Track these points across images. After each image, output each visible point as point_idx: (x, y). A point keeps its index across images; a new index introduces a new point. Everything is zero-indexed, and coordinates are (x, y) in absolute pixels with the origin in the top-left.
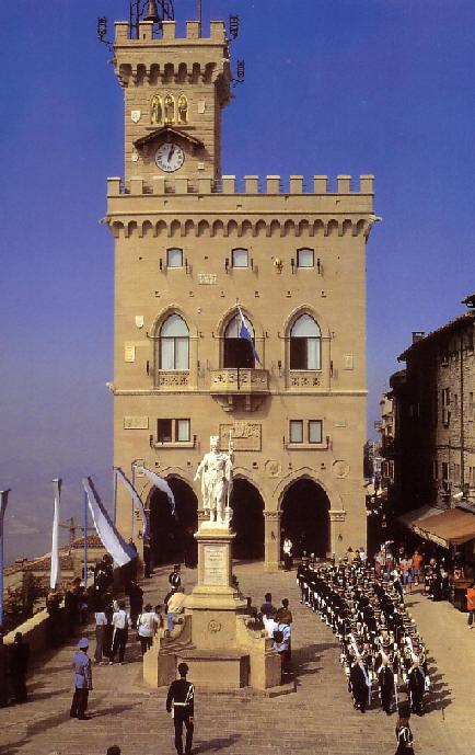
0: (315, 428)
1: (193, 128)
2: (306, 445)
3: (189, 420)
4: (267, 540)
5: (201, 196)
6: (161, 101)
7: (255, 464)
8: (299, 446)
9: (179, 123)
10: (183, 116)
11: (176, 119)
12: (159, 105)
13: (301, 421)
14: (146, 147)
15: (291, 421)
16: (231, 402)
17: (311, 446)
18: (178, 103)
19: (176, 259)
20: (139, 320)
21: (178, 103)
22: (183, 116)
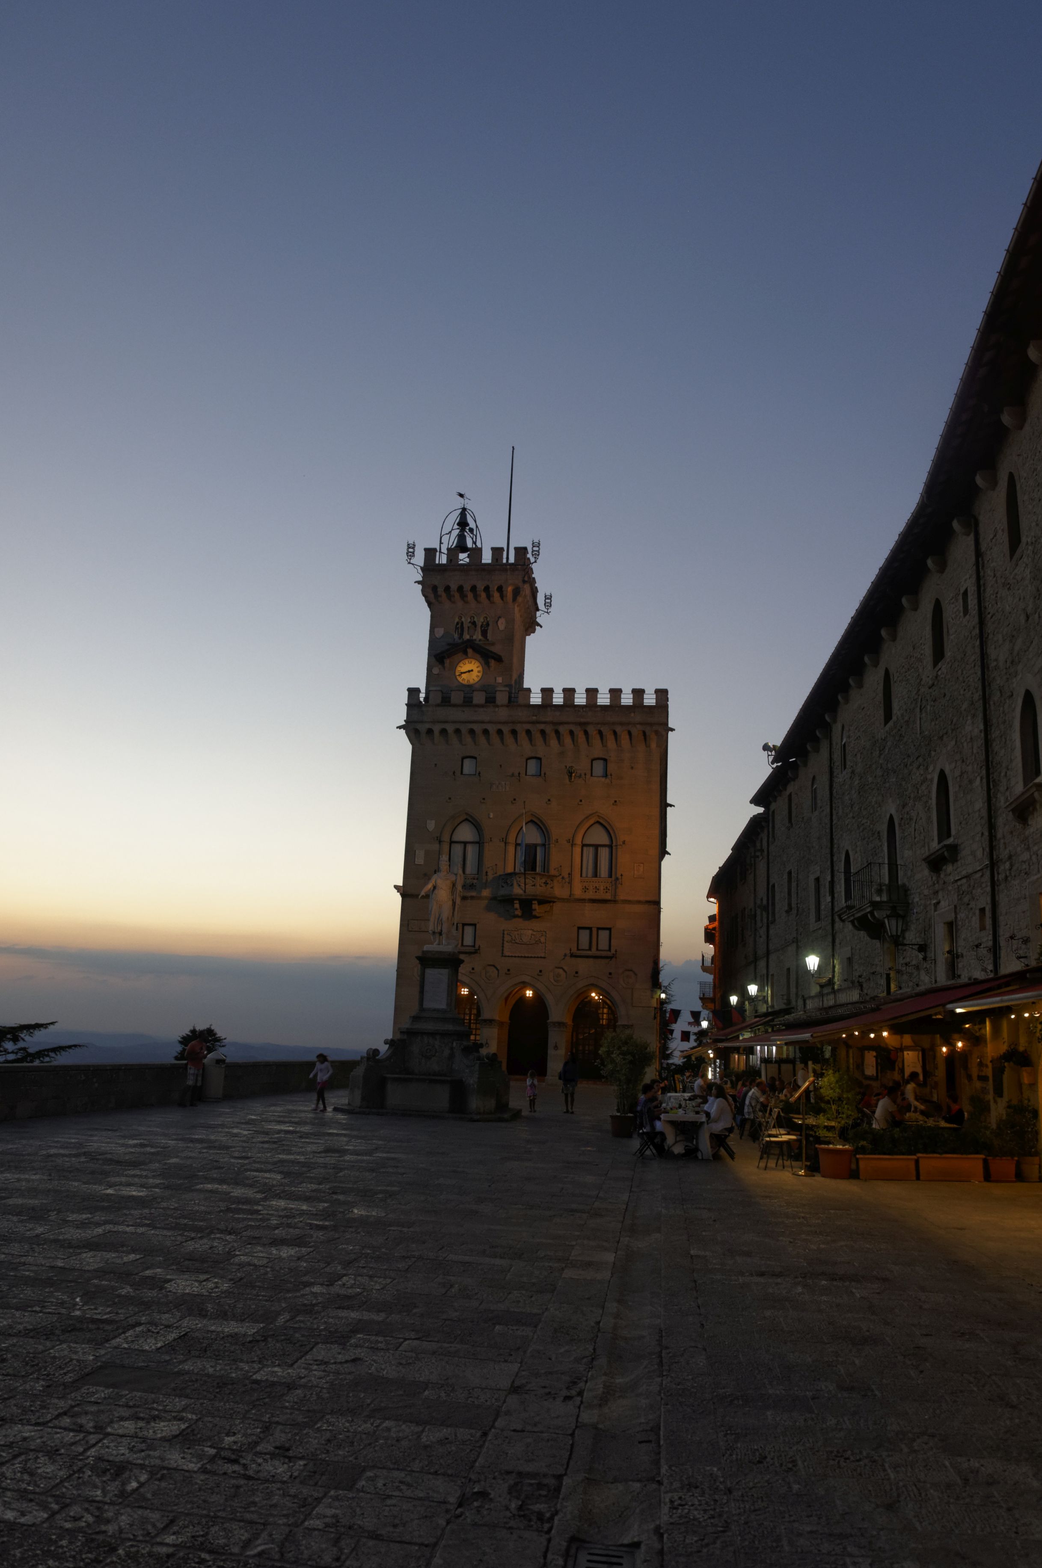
0: (604, 935)
1: (493, 644)
2: (594, 952)
3: (475, 925)
4: (551, 1052)
5: (498, 706)
6: (463, 619)
7: (541, 971)
8: (589, 953)
9: (480, 640)
10: (484, 633)
11: (478, 636)
12: (462, 623)
13: (590, 929)
14: (447, 662)
15: (579, 928)
16: (517, 906)
17: (599, 953)
18: (480, 621)
19: (469, 767)
20: (431, 825)
21: (480, 621)
22: (484, 633)
